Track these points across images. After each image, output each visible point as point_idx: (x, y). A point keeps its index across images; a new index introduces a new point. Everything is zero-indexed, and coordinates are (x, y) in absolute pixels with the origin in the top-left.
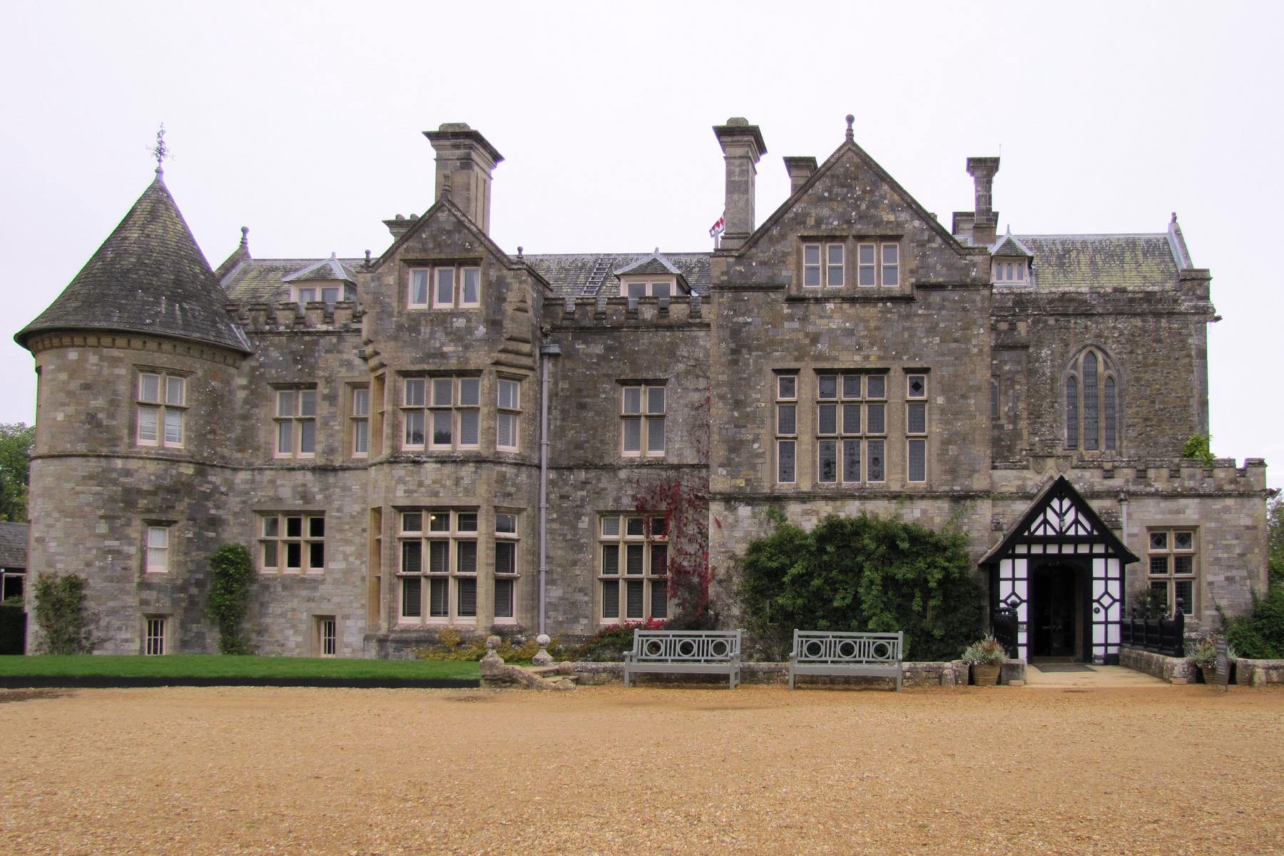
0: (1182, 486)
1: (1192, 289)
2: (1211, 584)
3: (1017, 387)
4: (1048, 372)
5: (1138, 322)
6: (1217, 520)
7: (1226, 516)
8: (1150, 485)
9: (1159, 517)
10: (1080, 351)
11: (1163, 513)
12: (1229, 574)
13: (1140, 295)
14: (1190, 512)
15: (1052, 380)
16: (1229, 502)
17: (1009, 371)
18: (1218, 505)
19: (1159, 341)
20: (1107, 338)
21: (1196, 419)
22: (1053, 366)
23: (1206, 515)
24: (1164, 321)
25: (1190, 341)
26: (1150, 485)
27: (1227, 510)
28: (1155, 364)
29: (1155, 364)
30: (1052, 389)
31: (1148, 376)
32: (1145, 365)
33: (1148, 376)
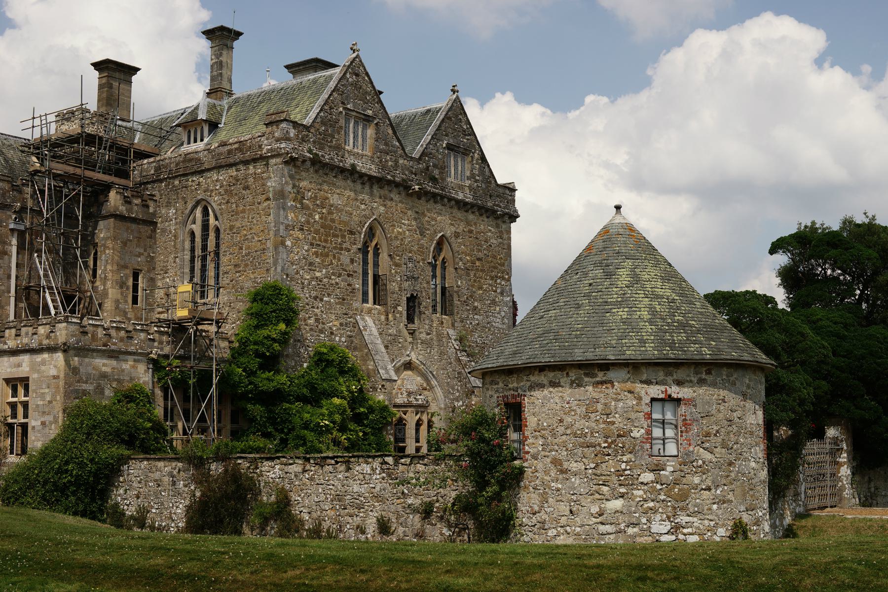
0: (21, 343)
1: (272, 133)
2: (33, 427)
3: (107, 252)
4: (173, 228)
5: (232, 172)
6: (38, 371)
7: (43, 368)
8: (5, 343)
9: (9, 370)
10: (195, 207)
11: (11, 367)
12: (43, 419)
13: (236, 146)
14: (24, 365)
15: (175, 236)
16: (46, 356)
17: (103, 238)
18: (39, 358)
19: (246, 188)
20: (212, 191)
21: (271, 261)
22: (176, 224)
23: (33, 367)
24: (251, 167)
25: (269, 184)
26: (5, 343)
27: (43, 363)
28: (243, 211)
29: (243, 211)
30: (175, 246)
31: (238, 224)
32: (237, 213)
33: (238, 224)
